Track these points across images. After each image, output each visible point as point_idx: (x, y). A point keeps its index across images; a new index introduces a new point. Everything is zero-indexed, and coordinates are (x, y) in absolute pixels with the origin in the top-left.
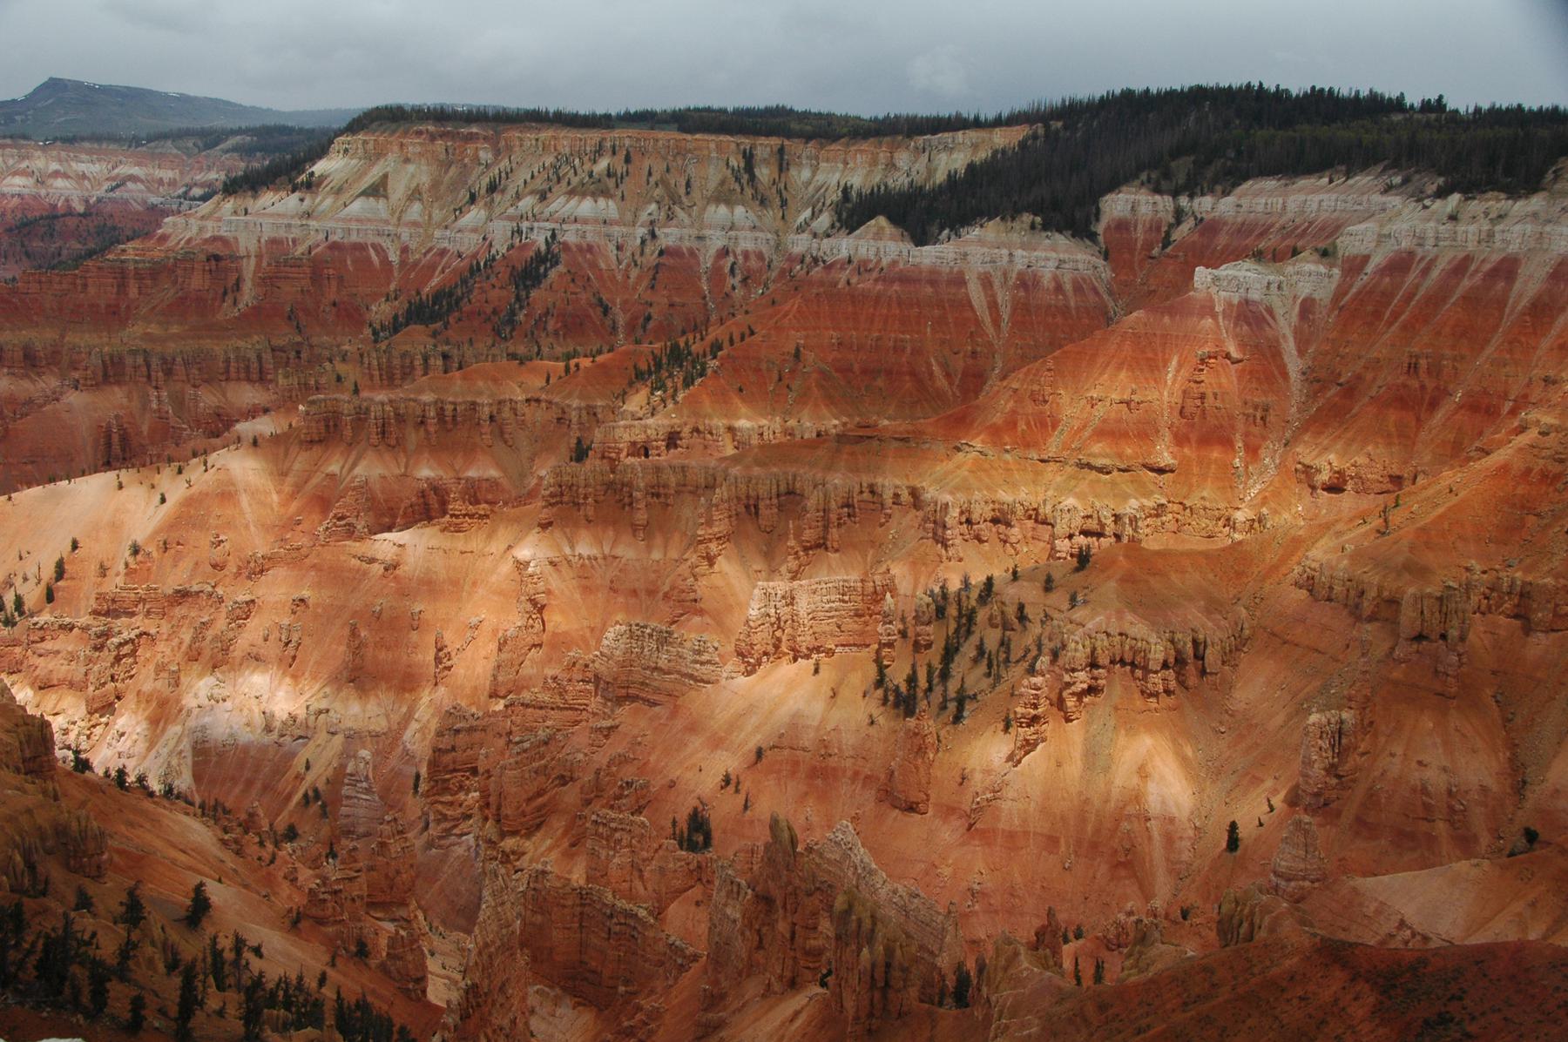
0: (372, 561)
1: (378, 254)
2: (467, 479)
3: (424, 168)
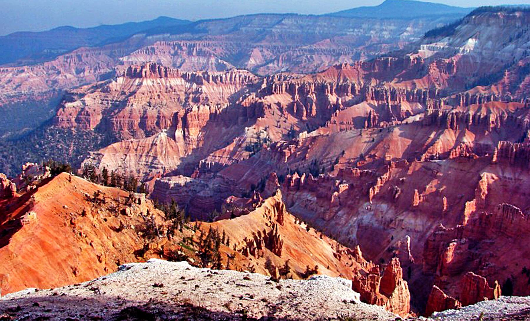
0: (430, 169)
1: (472, 59)
2: (480, 145)
3: (495, 28)
